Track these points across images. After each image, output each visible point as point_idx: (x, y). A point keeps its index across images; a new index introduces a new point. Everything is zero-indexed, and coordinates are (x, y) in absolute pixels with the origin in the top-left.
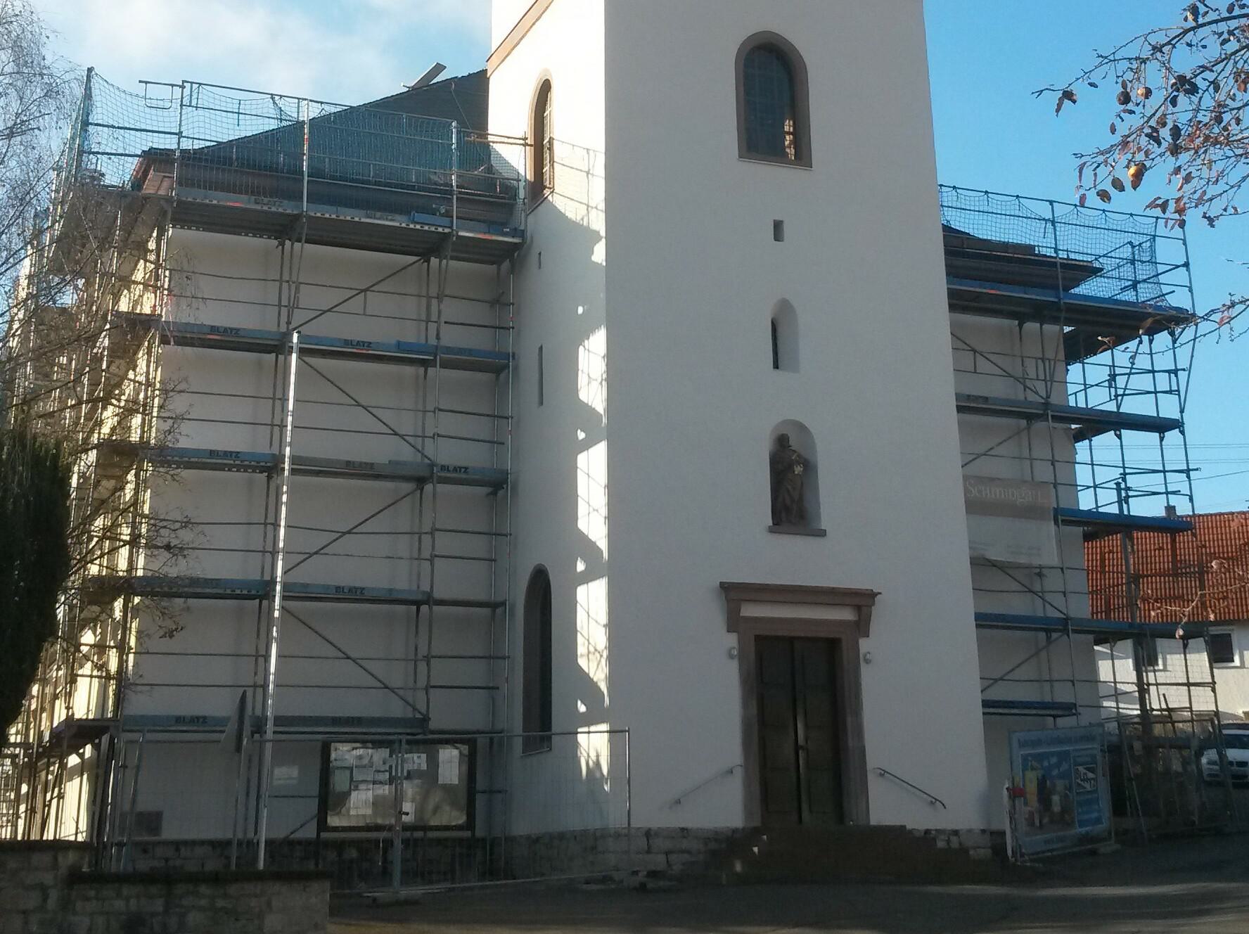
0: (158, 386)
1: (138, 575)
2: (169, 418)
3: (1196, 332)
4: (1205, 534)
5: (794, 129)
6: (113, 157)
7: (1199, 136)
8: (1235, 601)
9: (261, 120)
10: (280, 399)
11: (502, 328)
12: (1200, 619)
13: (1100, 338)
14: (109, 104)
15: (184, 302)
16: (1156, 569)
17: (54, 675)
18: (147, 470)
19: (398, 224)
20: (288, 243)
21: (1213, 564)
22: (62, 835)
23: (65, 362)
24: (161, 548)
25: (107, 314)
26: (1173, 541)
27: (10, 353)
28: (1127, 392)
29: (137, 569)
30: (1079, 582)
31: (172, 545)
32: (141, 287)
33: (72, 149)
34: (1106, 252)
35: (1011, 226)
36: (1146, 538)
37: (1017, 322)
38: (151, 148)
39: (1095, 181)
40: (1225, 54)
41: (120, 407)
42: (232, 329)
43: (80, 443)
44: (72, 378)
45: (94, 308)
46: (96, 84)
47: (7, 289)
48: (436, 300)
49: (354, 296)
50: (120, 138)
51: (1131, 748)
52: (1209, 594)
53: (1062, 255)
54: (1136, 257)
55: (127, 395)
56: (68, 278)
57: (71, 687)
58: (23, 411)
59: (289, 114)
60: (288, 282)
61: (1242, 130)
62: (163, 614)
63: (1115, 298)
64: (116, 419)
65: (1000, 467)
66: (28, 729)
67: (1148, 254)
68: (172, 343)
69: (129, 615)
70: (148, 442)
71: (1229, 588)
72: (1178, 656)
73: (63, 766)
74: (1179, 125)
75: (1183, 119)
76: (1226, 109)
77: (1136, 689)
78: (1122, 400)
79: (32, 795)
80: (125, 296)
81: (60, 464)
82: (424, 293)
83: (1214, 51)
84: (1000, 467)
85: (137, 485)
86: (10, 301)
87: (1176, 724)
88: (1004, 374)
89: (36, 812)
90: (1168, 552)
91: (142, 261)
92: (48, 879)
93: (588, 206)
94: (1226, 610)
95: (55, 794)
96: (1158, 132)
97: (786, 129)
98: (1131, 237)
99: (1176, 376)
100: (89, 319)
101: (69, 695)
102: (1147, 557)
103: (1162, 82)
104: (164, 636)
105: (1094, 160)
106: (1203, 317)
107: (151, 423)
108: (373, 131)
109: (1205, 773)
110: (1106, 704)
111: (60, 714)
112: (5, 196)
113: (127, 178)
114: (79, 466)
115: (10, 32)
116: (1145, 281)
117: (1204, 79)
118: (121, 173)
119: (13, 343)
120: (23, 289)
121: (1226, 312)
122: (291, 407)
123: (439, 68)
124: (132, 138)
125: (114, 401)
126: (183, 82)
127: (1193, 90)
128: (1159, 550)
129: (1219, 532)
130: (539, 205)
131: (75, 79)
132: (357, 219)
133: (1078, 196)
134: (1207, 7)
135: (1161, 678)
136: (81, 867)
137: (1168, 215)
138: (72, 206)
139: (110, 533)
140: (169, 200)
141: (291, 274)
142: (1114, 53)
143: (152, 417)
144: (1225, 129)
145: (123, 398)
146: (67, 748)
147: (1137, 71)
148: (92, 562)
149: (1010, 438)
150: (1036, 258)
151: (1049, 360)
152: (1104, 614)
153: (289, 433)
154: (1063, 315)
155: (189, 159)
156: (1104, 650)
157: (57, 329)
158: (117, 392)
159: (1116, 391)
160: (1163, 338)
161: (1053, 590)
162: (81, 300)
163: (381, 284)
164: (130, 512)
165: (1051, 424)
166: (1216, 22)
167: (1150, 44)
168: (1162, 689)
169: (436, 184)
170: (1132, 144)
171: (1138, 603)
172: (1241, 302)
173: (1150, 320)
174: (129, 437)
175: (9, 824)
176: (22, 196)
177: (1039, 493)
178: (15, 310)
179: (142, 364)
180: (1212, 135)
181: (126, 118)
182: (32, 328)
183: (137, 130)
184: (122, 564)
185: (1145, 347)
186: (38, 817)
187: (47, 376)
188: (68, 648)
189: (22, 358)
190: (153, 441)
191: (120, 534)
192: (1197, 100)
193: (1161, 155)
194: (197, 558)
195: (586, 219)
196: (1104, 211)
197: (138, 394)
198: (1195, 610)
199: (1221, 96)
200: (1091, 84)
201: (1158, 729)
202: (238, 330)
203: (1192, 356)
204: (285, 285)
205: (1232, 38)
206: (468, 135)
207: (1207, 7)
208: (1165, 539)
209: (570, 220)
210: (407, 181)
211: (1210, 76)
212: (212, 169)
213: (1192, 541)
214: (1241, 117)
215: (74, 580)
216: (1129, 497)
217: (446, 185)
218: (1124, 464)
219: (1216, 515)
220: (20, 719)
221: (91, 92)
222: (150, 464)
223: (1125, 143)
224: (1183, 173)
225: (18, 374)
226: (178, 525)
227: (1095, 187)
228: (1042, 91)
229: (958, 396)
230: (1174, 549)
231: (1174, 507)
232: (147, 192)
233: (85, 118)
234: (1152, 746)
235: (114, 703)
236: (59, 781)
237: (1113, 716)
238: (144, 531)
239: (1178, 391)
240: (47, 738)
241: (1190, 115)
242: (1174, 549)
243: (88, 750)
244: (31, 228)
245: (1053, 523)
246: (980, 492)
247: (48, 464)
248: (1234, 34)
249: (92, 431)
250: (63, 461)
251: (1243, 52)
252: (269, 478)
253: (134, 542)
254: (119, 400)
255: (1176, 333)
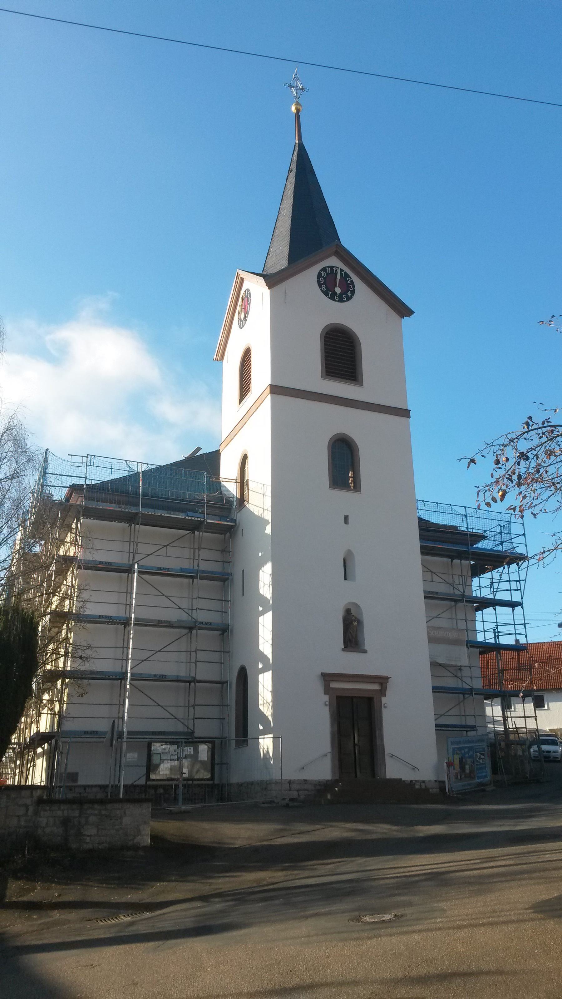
0: (76, 587)
1: (68, 669)
2: (81, 601)
3: (528, 564)
4: (532, 652)
5: (353, 475)
6: (57, 488)
7: (530, 479)
8: (545, 681)
9: (121, 472)
10: (129, 593)
11: (226, 562)
12: (530, 689)
13: (486, 566)
14: (55, 464)
15: (88, 551)
16: (511, 667)
17: (31, 713)
18: (71, 624)
19: (181, 517)
20: (133, 525)
21: (536, 665)
22: (35, 783)
23: (36, 577)
24: (78, 658)
25: (54, 556)
26: (518, 655)
27: (12, 573)
28: (498, 590)
29: (67, 667)
30: (477, 672)
31: (83, 656)
32: (69, 544)
33: (39, 484)
34: (489, 529)
35: (448, 518)
36: (506, 654)
37: (450, 560)
38: (73, 484)
39: (484, 498)
40: (541, 443)
41: (60, 597)
42: (109, 563)
43: (43, 612)
44: (39, 584)
45: (49, 553)
46: (49, 455)
47: (11, 545)
48: (198, 550)
49: (162, 548)
50: (60, 479)
51: (500, 745)
52: (534, 678)
53: (470, 530)
54: (502, 531)
55: (63, 591)
56: (37, 540)
57: (38, 718)
58: (18, 598)
59: (134, 469)
60: (133, 542)
61: (548, 476)
62: (79, 686)
63: (493, 549)
64: (58, 601)
65: (443, 623)
66: (20, 737)
67: (507, 530)
68: (83, 569)
69: (64, 687)
70: (72, 612)
71: (543, 675)
72: (520, 705)
73: (35, 753)
74: (521, 474)
75: (523, 471)
76: (541, 467)
77: (502, 719)
78: (496, 594)
79: (22, 765)
80: (62, 548)
81: (34, 621)
82: (192, 547)
83: (536, 441)
84: (443, 623)
85: (67, 630)
86: (12, 550)
87: (520, 734)
88: (445, 582)
89: (23, 773)
90: (516, 660)
91: (69, 533)
92: (29, 802)
93: (264, 509)
94: (541, 685)
95: (32, 765)
96: (511, 477)
97: (350, 475)
98: (500, 523)
99: (520, 583)
100: (47, 558)
101: (38, 722)
102: (507, 662)
103: (513, 455)
104: (79, 696)
105: (484, 489)
106: (531, 557)
107: (73, 603)
108: (170, 476)
109: (532, 756)
110: (489, 726)
111: (34, 730)
112: (10, 505)
113: (63, 497)
114: (42, 622)
115: (12, 433)
116: (506, 541)
117: (532, 454)
118: (60, 494)
119: (14, 569)
120: (18, 545)
121: (541, 555)
122: (134, 596)
123: (199, 449)
124: (65, 479)
125: (57, 594)
126: (87, 455)
127: (527, 458)
128: (512, 659)
129: (538, 651)
130: (242, 508)
131: (40, 454)
132: (163, 515)
133: (477, 505)
134: (533, 422)
135: (513, 714)
136: (43, 797)
137: (516, 513)
138: (39, 509)
139: (56, 651)
140: (81, 506)
141: (134, 538)
142: (492, 442)
143: (74, 601)
144: (541, 475)
145: (61, 592)
146: (37, 744)
147: (502, 450)
148: (48, 664)
149: (447, 610)
150: (459, 532)
151: (464, 576)
152: (488, 686)
153: (133, 608)
154: (470, 556)
155: (90, 488)
156: (488, 702)
157: (32, 562)
158: (59, 590)
159: (493, 590)
160: (514, 567)
161: (466, 676)
162: (43, 550)
163: (173, 543)
164: (64, 642)
165: (465, 604)
166: (537, 429)
167: (508, 438)
168: (514, 719)
169: (197, 499)
170: (500, 482)
171: (503, 682)
172: (548, 551)
173: (508, 559)
174: (64, 609)
175: (12, 778)
176: (17, 505)
177: (460, 634)
178: (14, 554)
179: (69, 578)
180: (535, 478)
181: (62, 471)
182: (22, 562)
183: (67, 476)
184: (61, 665)
185: (506, 570)
186: (24, 775)
187: (28, 583)
188: (37, 701)
189: (17, 575)
190: (74, 611)
191: (60, 652)
192: (529, 463)
193: (513, 487)
194: (93, 662)
195: (263, 515)
196: (488, 511)
197: (68, 591)
198: (528, 684)
199: (539, 461)
200: (482, 456)
201: (512, 737)
202: (111, 563)
203: (527, 574)
204: (132, 543)
205: (544, 436)
206: (212, 478)
207: (533, 422)
208: (515, 654)
209: (256, 515)
210: (185, 498)
211: (534, 452)
212: (100, 493)
213: (527, 655)
214: (548, 470)
215: (40, 672)
216: (499, 635)
217: (202, 500)
218: (497, 621)
219: (537, 643)
220: (16, 732)
221: (47, 460)
222: (73, 621)
223: (497, 482)
224: (523, 495)
225: (15, 582)
226: (85, 648)
227: (484, 501)
228: (461, 459)
229: (425, 592)
230: (519, 658)
231: (519, 640)
232: (72, 503)
233: (45, 471)
234: (509, 744)
235: (57, 725)
236: (33, 759)
237: (492, 731)
238: (70, 650)
239: (520, 589)
240: (28, 740)
241: (526, 469)
242: (519, 658)
243: (46, 746)
244: (21, 518)
245: (466, 647)
246: (434, 633)
247: (28, 621)
248: (545, 434)
249: (48, 607)
250: (35, 620)
251: (548, 442)
252: (125, 627)
253: (66, 655)
254: (59, 594)
255: (520, 564)
